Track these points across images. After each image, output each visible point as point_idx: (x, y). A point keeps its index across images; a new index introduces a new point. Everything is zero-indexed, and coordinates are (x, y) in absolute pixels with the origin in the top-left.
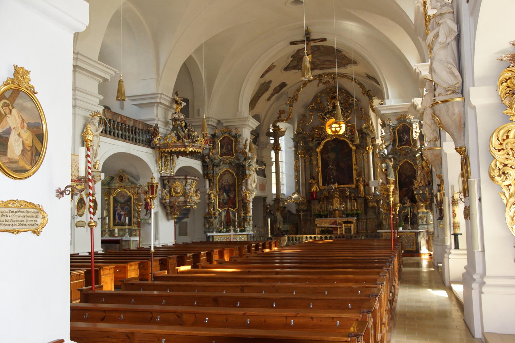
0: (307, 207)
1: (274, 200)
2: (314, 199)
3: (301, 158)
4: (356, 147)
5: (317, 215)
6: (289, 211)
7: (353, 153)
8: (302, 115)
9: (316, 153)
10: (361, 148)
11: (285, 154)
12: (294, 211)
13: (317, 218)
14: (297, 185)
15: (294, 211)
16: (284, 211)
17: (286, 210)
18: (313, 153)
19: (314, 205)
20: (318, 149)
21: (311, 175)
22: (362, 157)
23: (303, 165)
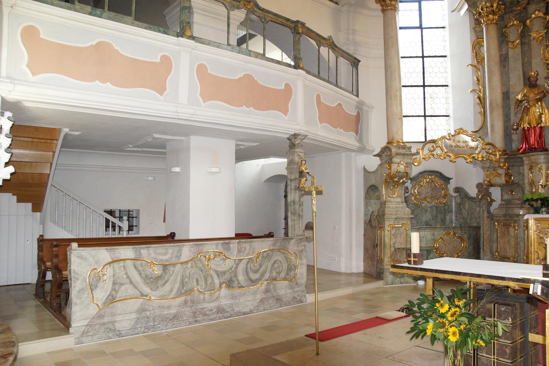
0: (508, 175)
1: (377, 151)
2: (532, 149)
5: (536, 200)
6: (458, 190)
12: (473, 192)
13: (537, 211)
14: (480, 113)
15: (473, 192)
16: (446, 189)
17: (452, 186)
19: (531, 169)
21: (524, 75)
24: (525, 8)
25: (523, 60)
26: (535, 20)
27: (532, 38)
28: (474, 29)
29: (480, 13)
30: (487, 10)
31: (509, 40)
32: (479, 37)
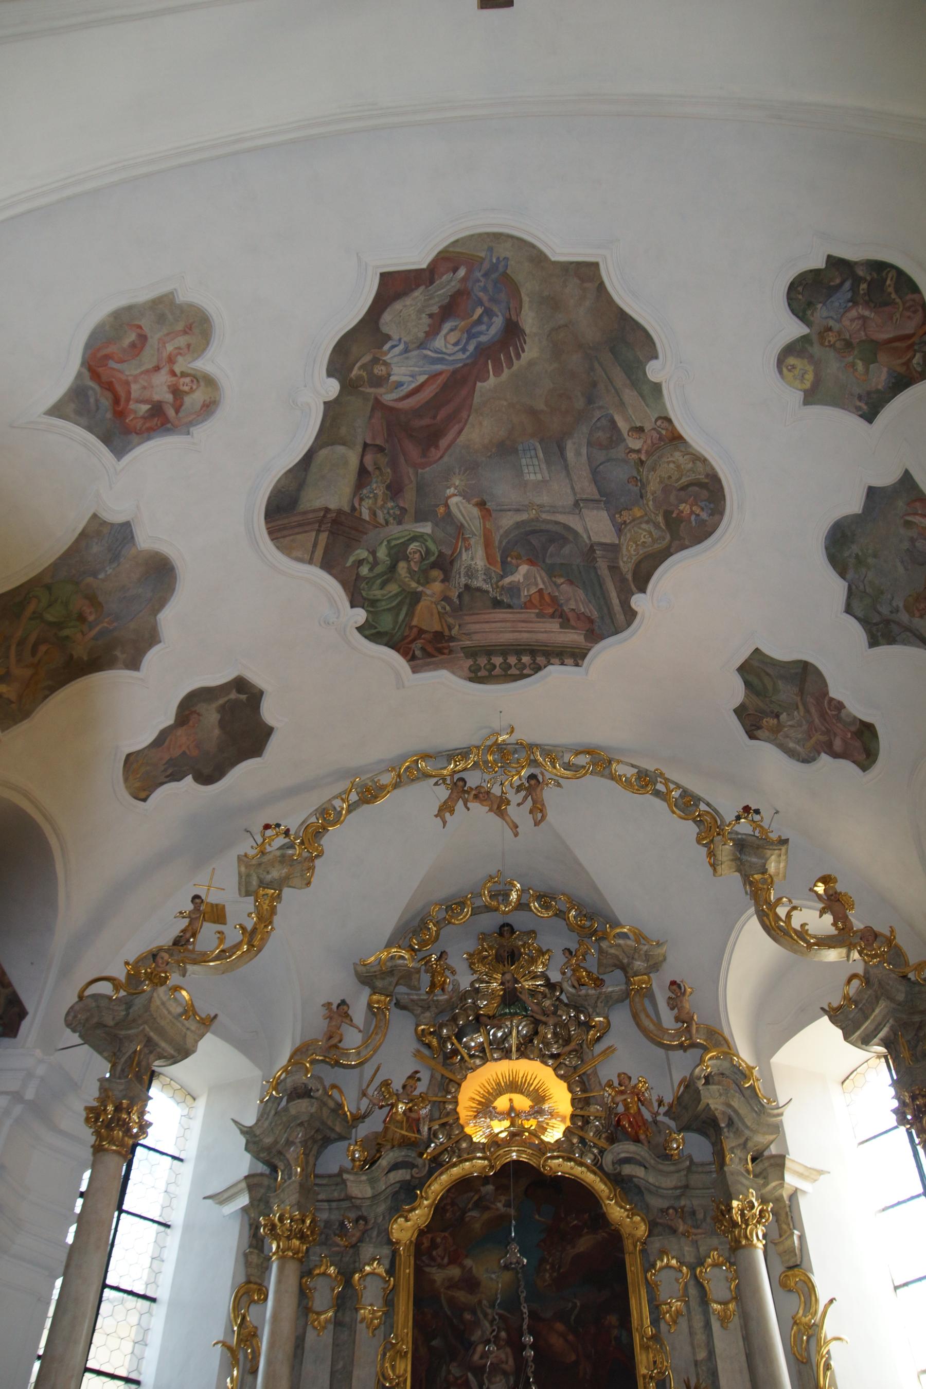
3: (283, 1259)
4: (653, 1226)
7: (633, 1267)
8: (328, 1005)
9: (386, 1251)
10: (681, 1228)
11: (182, 1247)
18: (368, 1251)
20: (401, 1220)
22: (693, 1291)
23: (287, 1328)
24: (354, 1246)
25: (334, 1363)
26: (369, 1279)
27: (359, 1319)
28: (246, 1255)
29: (273, 1227)
30: (291, 1226)
31: (310, 1304)
32: (253, 1279)
